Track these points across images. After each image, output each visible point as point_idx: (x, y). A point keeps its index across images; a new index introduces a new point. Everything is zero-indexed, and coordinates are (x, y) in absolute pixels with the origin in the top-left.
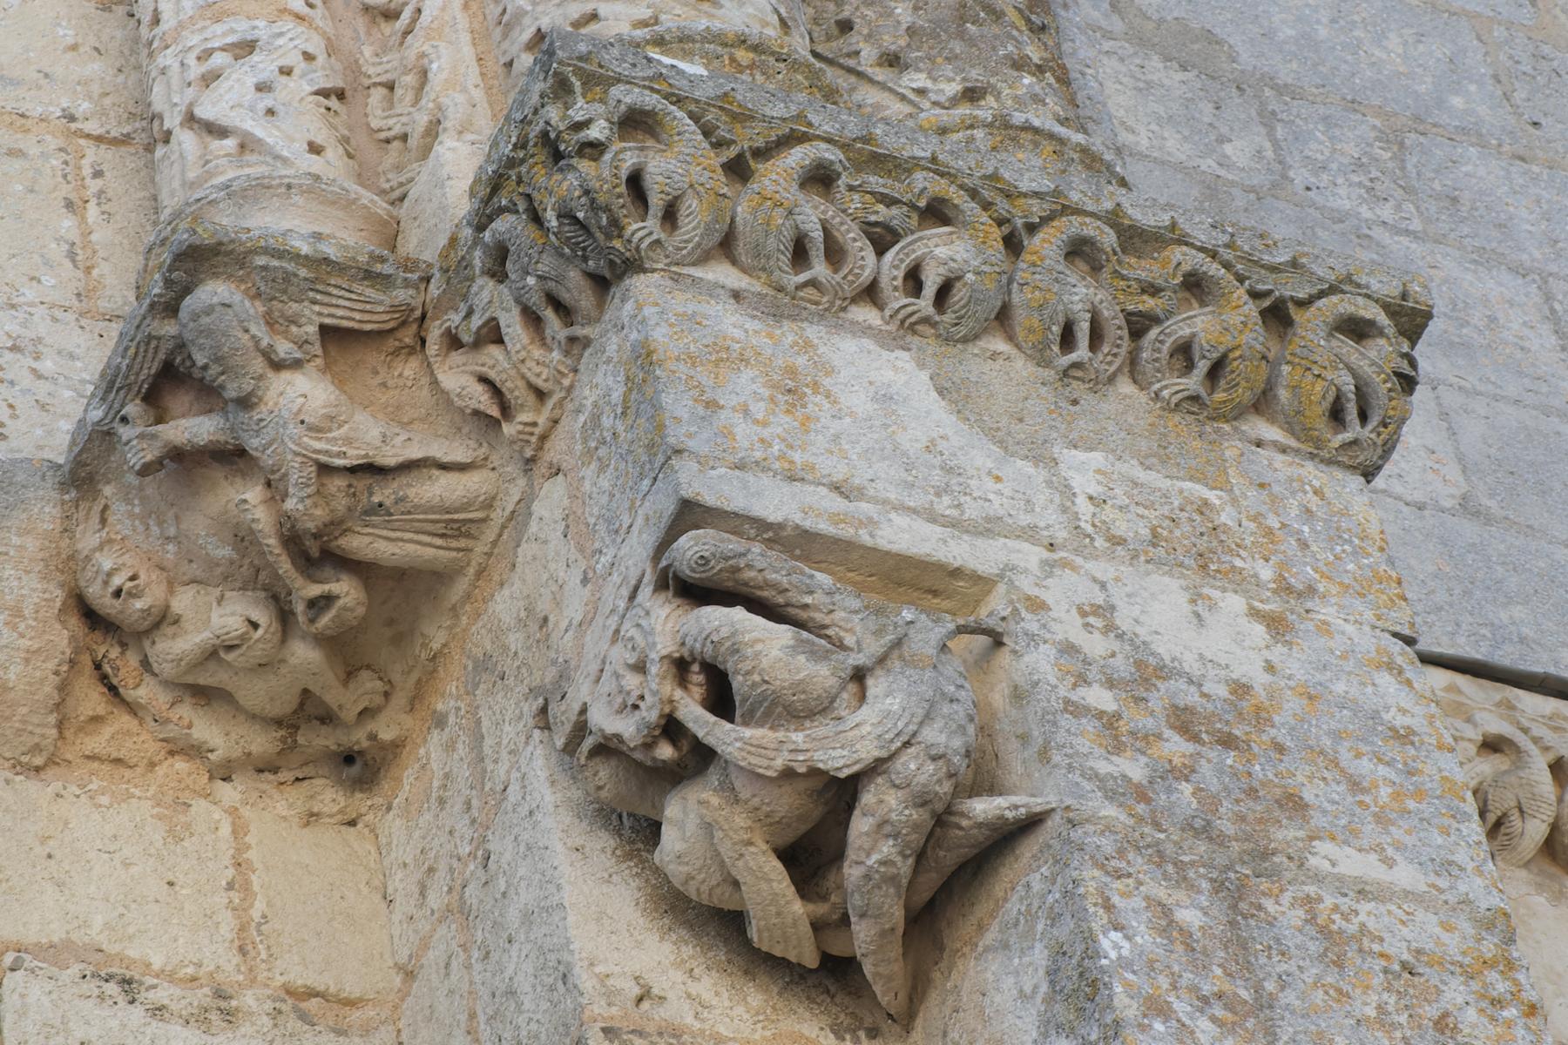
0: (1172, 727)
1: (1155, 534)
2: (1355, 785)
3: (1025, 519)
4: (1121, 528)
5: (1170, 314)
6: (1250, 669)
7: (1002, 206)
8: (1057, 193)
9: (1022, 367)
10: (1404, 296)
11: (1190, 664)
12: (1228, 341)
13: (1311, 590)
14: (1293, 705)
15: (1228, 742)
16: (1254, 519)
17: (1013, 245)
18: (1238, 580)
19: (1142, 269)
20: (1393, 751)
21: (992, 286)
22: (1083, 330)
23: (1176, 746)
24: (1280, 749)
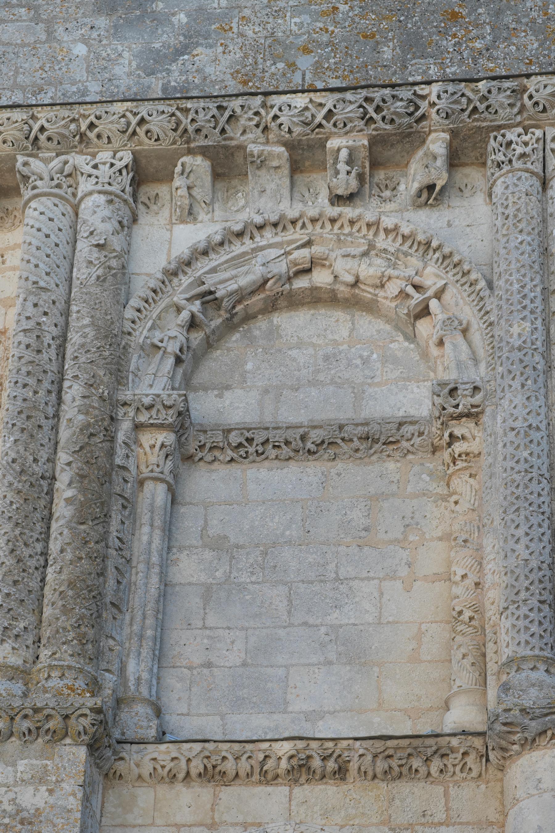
0: (19, 823)
1: (32, 776)
2: (54, 826)
3: (5, 781)
4: (25, 778)
5: (44, 725)
6: (41, 805)
7: (10, 712)
8: (23, 705)
9: (18, 742)
10: (96, 704)
11: (29, 807)
12: (54, 728)
13: (62, 780)
14: (47, 810)
15: (30, 823)
16: (56, 766)
17: (12, 719)
18: (46, 782)
19: (39, 716)
20: (65, 815)
21: (7, 731)
22: (26, 733)
23: (19, 827)
24: (41, 822)
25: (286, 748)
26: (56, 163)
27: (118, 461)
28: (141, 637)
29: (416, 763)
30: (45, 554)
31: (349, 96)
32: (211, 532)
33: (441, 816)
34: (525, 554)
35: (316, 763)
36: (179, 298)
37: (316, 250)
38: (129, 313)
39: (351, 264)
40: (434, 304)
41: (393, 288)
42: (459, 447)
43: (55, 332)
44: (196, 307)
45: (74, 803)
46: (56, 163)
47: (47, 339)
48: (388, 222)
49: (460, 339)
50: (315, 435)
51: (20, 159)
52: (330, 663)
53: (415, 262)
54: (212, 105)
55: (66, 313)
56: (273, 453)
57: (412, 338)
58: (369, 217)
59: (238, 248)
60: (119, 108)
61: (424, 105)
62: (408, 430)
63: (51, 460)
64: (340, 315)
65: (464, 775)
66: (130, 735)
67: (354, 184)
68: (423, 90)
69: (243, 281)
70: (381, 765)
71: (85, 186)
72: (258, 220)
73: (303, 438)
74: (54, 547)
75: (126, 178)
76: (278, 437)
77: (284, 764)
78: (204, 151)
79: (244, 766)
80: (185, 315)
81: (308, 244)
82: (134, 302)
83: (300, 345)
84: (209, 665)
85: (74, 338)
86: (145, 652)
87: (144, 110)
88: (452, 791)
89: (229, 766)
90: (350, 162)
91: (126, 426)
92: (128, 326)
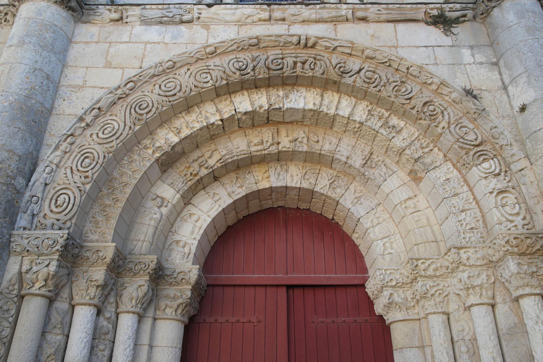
65: (6, 23)
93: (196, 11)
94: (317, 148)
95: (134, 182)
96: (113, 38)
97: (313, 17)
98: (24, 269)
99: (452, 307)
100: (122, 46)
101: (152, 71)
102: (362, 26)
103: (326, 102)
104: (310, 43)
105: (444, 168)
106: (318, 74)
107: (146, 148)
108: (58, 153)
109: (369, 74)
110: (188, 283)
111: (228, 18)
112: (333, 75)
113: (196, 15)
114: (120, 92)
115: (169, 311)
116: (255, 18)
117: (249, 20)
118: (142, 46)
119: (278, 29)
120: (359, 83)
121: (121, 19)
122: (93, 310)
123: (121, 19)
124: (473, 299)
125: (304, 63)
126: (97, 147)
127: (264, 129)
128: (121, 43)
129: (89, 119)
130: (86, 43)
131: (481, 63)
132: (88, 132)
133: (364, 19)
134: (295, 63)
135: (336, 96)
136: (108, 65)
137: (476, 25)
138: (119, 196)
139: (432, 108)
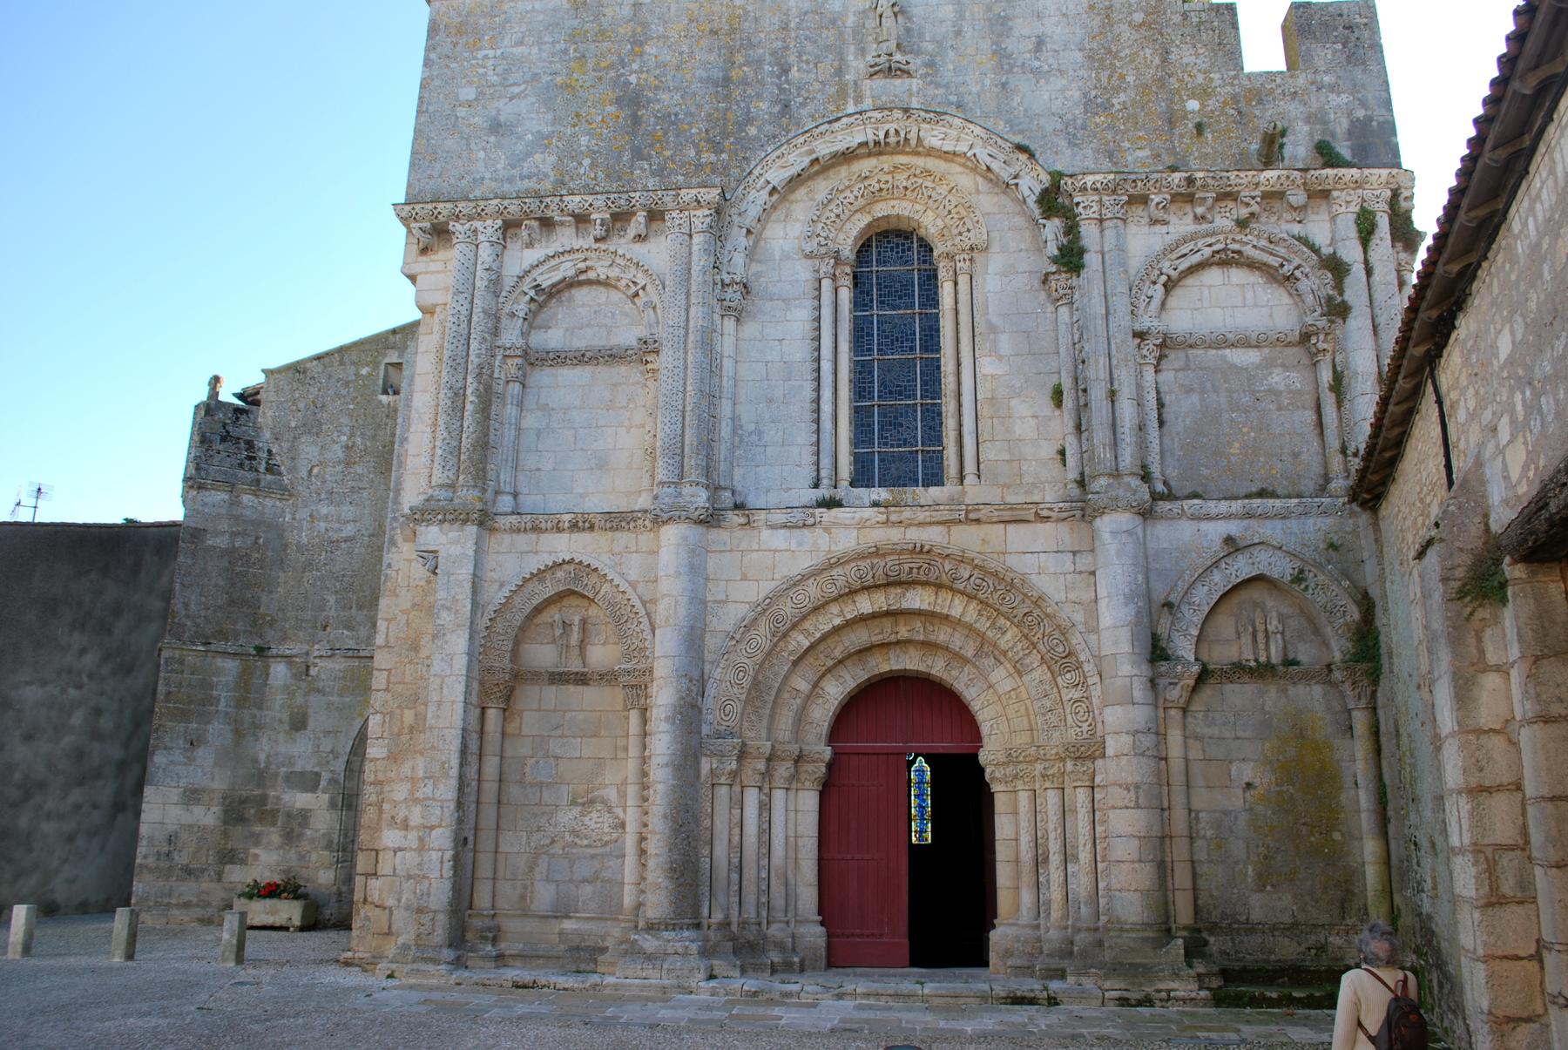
25: (567, 518)
26: (467, 226)
27: (496, 375)
28: (507, 461)
29: (623, 524)
30: (462, 426)
31: (599, 196)
32: (541, 402)
33: (634, 549)
34: (668, 431)
35: (580, 524)
36: (525, 289)
37: (588, 263)
38: (501, 300)
39: (605, 270)
40: (641, 292)
41: (623, 283)
42: (650, 366)
43: (466, 313)
44: (532, 293)
45: (471, 553)
46: (467, 226)
47: (462, 318)
48: (620, 252)
49: (651, 312)
50: (588, 354)
51: (451, 223)
52: (592, 469)
53: (633, 270)
54: (537, 201)
55: (472, 302)
56: (568, 362)
57: (634, 303)
58: (612, 249)
59: (553, 262)
60: (496, 201)
61: (634, 201)
62: (630, 352)
63: (465, 379)
64: (602, 289)
66: (500, 511)
67: (604, 234)
68: (632, 195)
69: (555, 280)
70: (608, 525)
71: (481, 237)
72: (561, 250)
73: (583, 355)
74: (465, 425)
75: (500, 232)
76: (571, 355)
77: (567, 525)
78: (535, 219)
79: (549, 525)
80: (528, 297)
81: (585, 260)
82: (504, 294)
83: (584, 305)
84: (539, 470)
85: (475, 318)
86: (509, 469)
87: (506, 203)
88: (640, 537)
89: (543, 525)
90: (602, 225)
91: (499, 358)
92: (500, 306)
93: (818, 515)
94: (932, 638)
95: (777, 685)
96: (744, 546)
97: (928, 520)
98: (714, 766)
99: (1037, 787)
100: (754, 555)
101: (784, 586)
102: (974, 528)
103: (939, 601)
104: (925, 549)
105: (1039, 671)
106: (932, 580)
107: (783, 651)
108: (719, 670)
109: (978, 582)
110: (822, 761)
111: (848, 522)
112: (945, 579)
113: (818, 519)
114: (759, 609)
115: (807, 784)
116: (873, 521)
117: (868, 524)
118: (770, 555)
119: (894, 535)
120: (969, 589)
121: (749, 523)
122: (757, 790)
123: (749, 523)
124: (1048, 784)
125: (919, 568)
126: (747, 661)
127: (884, 620)
128: (752, 551)
129: (738, 637)
130: (721, 552)
131: (1081, 572)
132: (739, 647)
133: (978, 521)
134: (911, 569)
135: (950, 594)
136: (744, 578)
137: (1083, 525)
138: (767, 698)
139: (1030, 618)
